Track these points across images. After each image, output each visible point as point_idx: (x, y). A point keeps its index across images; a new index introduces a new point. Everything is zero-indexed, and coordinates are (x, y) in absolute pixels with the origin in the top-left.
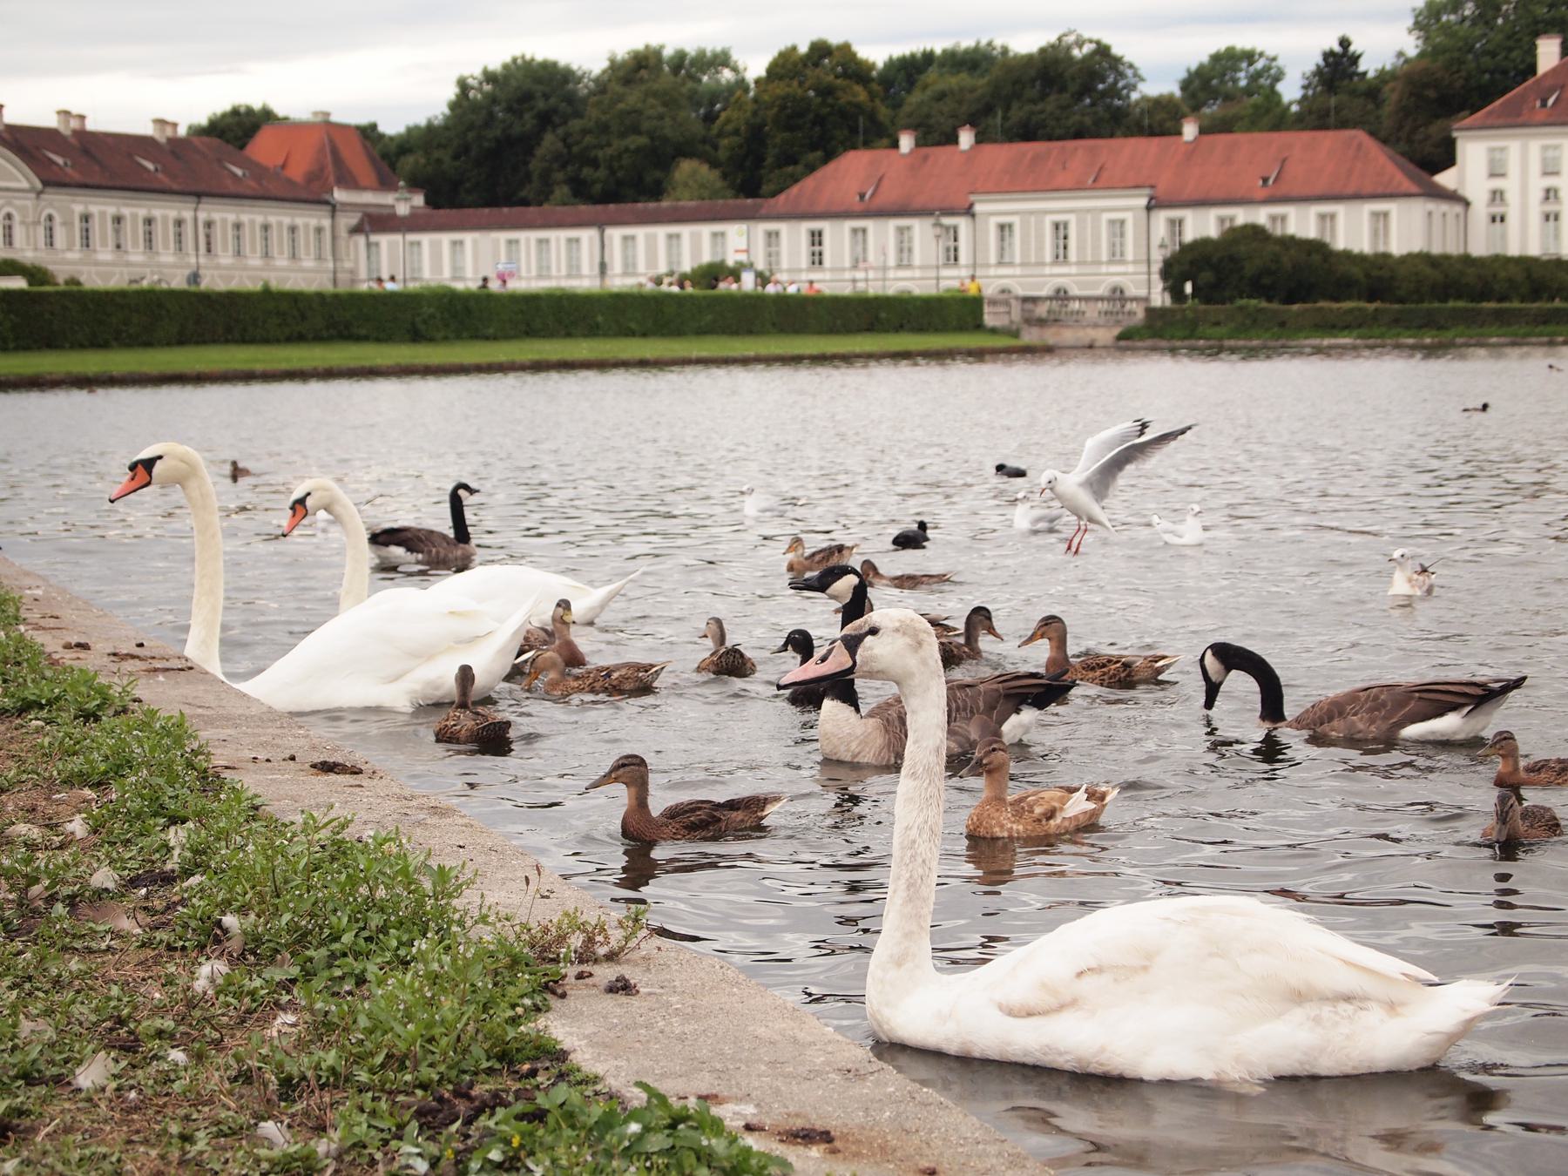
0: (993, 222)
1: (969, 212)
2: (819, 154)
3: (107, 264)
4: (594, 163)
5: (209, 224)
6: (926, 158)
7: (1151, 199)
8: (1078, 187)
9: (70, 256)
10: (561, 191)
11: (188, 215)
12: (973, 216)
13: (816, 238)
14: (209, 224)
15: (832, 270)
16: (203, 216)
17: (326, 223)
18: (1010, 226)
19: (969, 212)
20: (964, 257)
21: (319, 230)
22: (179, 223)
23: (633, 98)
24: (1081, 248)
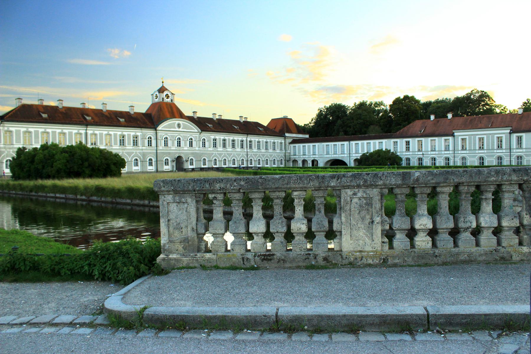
0: (460, 138)
1: (453, 135)
2: (407, 122)
3: (221, 151)
4: (350, 127)
5: (251, 142)
6: (438, 121)
7: (511, 130)
8: (486, 127)
9: (209, 149)
10: (341, 133)
11: (245, 139)
12: (454, 136)
13: (408, 143)
14: (251, 142)
15: (412, 152)
16: (249, 139)
17: (283, 141)
18: (465, 139)
19: (453, 135)
20: (451, 148)
21: (281, 143)
22: (242, 141)
23: (360, 111)
24: (488, 145)
